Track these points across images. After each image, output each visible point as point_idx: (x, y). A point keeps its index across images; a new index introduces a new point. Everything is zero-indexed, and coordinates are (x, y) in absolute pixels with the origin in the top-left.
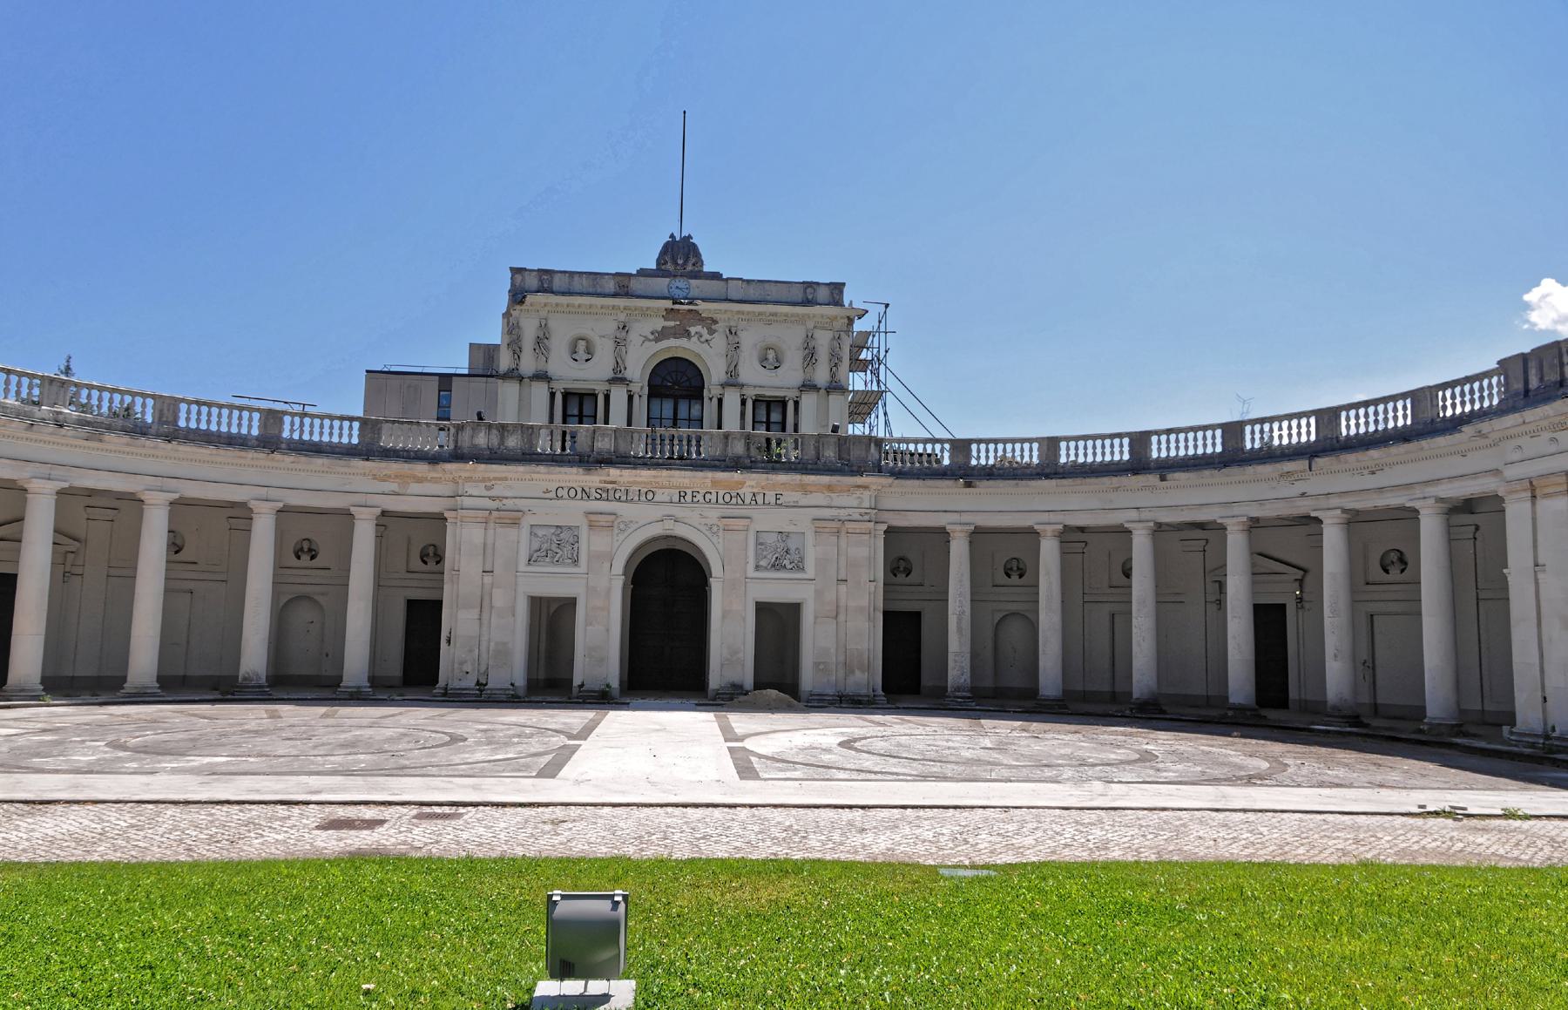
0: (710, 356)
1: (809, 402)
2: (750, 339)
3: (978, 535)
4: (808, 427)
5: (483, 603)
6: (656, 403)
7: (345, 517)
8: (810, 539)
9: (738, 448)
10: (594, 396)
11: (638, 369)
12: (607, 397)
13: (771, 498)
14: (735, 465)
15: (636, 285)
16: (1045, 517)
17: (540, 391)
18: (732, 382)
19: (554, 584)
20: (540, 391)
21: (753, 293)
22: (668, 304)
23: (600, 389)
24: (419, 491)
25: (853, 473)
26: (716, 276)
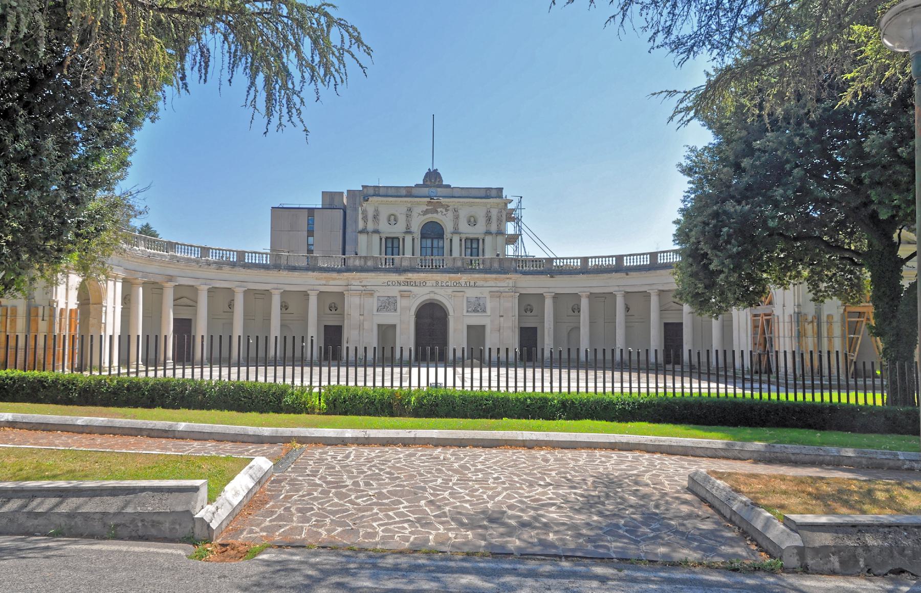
0: (446, 221)
1: (488, 239)
2: (464, 213)
3: (556, 297)
4: (488, 255)
5: (360, 327)
6: (424, 240)
7: (305, 295)
8: (488, 300)
9: (459, 264)
10: (398, 238)
11: (416, 227)
12: (404, 240)
13: (472, 284)
14: (456, 271)
15: (414, 192)
16: (582, 289)
17: (376, 238)
18: (456, 232)
19: (387, 318)
20: (376, 238)
21: (464, 193)
22: (428, 199)
23: (401, 236)
24: (335, 283)
25: (505, 273)
26: (448, 186)
